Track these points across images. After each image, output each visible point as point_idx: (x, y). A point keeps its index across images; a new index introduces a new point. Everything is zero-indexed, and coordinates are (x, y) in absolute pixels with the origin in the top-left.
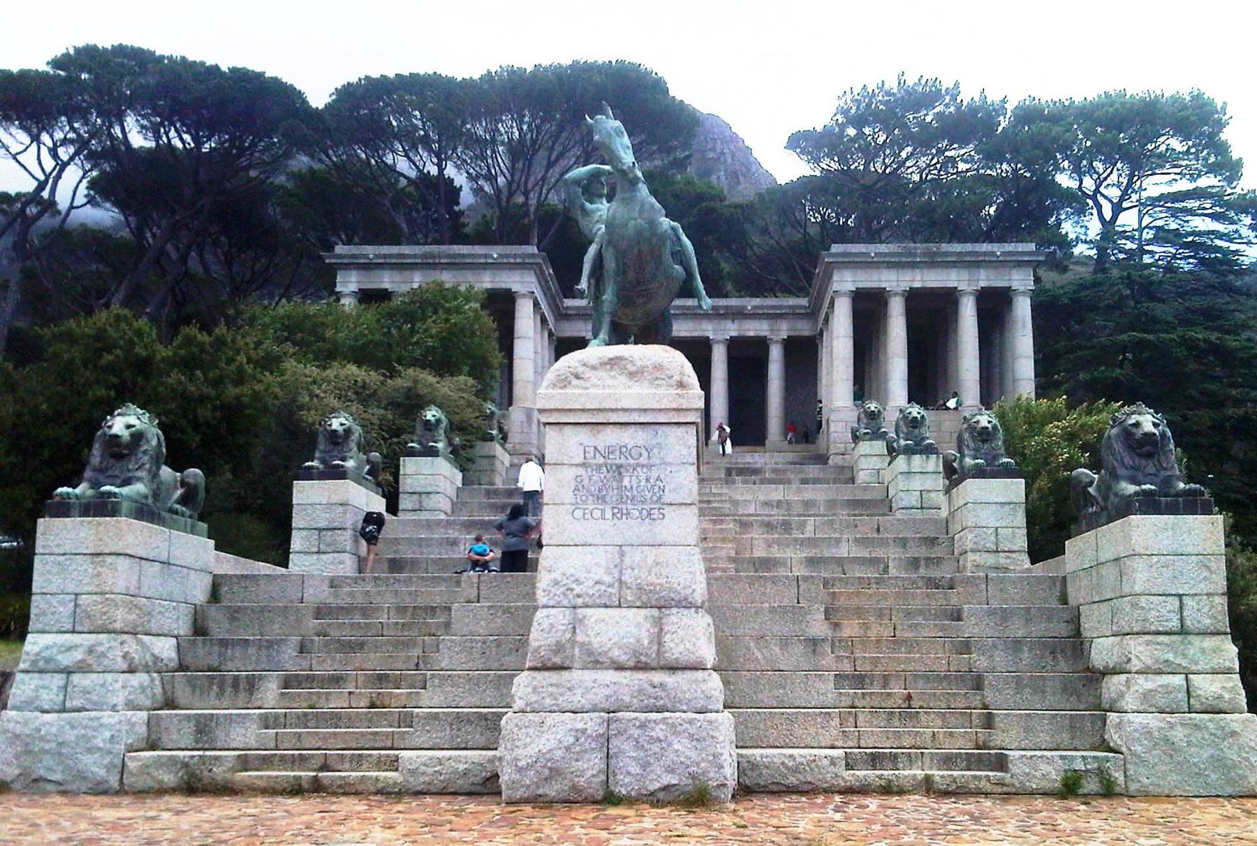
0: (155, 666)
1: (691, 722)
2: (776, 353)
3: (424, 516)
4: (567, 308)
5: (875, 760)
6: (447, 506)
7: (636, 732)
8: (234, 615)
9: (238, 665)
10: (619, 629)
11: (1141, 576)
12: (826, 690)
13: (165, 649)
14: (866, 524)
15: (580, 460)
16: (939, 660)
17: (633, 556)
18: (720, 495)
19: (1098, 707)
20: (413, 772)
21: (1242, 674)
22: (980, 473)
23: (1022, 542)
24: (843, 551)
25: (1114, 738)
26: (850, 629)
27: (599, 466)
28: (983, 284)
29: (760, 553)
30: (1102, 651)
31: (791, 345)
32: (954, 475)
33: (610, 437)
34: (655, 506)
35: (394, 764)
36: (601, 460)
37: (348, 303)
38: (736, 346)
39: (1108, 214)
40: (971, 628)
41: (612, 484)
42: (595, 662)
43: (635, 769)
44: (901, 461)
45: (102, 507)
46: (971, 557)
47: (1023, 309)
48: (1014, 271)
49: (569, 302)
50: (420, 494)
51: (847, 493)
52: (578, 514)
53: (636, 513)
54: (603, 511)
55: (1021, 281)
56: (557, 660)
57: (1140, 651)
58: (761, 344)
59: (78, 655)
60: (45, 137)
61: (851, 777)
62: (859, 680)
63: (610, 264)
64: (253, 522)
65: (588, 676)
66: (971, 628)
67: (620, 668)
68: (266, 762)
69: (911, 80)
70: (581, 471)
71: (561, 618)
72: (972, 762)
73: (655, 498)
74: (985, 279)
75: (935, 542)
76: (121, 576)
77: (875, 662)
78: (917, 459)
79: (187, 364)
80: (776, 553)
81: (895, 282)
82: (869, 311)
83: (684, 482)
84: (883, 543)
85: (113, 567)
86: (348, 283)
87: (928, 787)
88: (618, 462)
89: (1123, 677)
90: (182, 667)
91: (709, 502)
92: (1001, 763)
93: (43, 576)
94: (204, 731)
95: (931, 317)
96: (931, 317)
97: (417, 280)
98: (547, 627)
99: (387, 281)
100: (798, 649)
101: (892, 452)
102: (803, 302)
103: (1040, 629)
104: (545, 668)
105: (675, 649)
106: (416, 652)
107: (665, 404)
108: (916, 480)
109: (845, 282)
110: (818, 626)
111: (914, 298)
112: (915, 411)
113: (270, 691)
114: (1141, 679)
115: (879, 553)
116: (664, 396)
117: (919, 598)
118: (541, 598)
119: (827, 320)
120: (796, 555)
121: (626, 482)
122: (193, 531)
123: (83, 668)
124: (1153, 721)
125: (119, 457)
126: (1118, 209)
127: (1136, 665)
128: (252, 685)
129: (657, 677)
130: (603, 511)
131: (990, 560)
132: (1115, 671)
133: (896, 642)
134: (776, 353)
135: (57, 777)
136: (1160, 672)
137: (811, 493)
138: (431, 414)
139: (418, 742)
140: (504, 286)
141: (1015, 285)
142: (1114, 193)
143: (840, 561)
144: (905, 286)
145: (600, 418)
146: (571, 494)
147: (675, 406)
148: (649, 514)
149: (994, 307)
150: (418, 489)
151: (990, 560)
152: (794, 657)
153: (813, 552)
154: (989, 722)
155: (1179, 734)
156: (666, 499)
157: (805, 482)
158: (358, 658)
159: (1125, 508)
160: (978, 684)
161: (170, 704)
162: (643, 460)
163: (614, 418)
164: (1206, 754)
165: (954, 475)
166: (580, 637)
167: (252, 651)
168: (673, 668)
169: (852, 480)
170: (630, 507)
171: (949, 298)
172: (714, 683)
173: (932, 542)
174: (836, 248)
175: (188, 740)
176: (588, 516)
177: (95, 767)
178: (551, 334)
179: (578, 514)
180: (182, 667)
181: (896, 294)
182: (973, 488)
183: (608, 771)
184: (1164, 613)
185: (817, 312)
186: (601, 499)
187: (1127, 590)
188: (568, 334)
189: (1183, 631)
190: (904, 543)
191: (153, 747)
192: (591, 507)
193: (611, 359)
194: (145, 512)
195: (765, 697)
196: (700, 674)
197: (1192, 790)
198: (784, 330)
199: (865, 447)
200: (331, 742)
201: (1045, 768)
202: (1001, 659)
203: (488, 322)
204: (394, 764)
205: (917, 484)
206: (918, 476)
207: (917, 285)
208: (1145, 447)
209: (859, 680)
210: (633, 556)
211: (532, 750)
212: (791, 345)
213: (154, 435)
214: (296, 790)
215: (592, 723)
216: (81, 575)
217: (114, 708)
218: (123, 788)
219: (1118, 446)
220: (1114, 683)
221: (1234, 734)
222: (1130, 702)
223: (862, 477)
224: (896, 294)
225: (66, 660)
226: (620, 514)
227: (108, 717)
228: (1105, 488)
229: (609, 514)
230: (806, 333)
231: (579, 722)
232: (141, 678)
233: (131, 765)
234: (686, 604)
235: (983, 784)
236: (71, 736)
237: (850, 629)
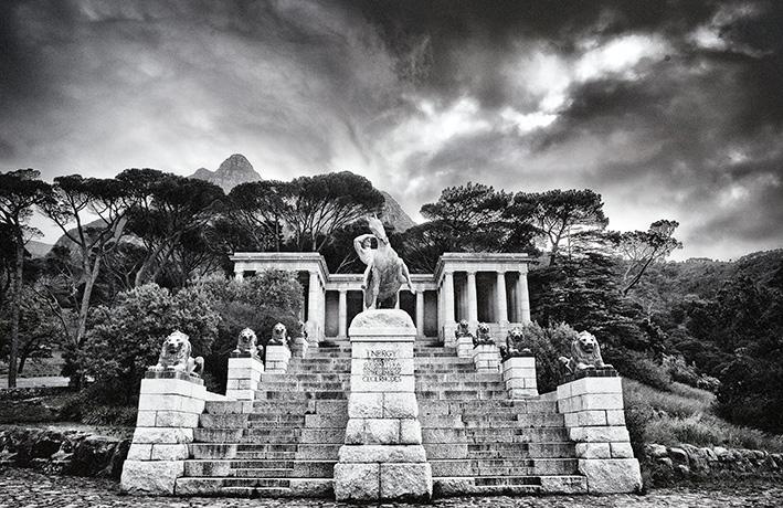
0: (186, 442)
1: (414, 467)
3: (276, 372)
5: (487, 481)
6: (285, 367)
7: (391, 471)
8: (215, 418)
9: (220, 439)
10: (384, 428)
11: (590, 402)
12: (465, 451)
13: (189, 434)
14: (469, 377)
16: (509, 437)
17: (388, 397)
19: (574, 457)
20: (296, 488)
21: (631, 441)
22: (517, 355)
23: (535, 385)
24: (460, 388)
25: (582, 469)
26: (472, 425)
29: (425, 390)
30: (575, 434)
31: (426, 293)
32: (505, 356)
33: (379, 347)
34: (395, 375)
35: (287, 484)
37: (239, 277)
39: (555, 240)
40: (521, 423)
41: (382, 367)
42: (373, 442)
43: (391, 487)
44: (480, 346)
45: (168, 374)
46: (514, 391)
47: (523, 280)
49: (331, 276)
51: (455, 361)
55: (523, 269)
56: (358, 441)
57: (592, 433)
59: (158, 437)
60: (113, 206)
61: (476, 489)
62: (478, 447)
63: (376, 275)
64: (216, 378)
65: (371, 448)
66: (521, 423)
67: (384, 444)
68: (233, 483)
71: (359, 423)
72: (526, 481)
75: (499, 385)
76: (175, 403)
77: (484, 439)
78: (486, 346)
79: (182, 306)
80: (432, 389)
81: (471, 269)
82: (460, 278)
83: (409, 365)
84: (477, 384)
85: (173, 401)
86: (239, 268)
87: (507, 492)
89: (584, 444)
90: (195, 441)
92: (538, 481)
93: (145, 402)
94: (207, 468)
95: (486, 282)
96: (486, 282)
97: (269, 266)
98: (353, 428)
99: (255, 267)
100: (451, 434)
101: (476, 344)
102: (432, 276)
103: (548, 424)
104: (353, 444)
105: (407, 437)
106: (291, 436)
108: (488, 357)
109: (449, 269)
110: (459, 424)
112: (484, 325)
113: (233, 452)
114: (592, 445)
115: (475, 389)
116: (401, 331)
117: (500, 411)
118: (350, 414)
119: (442, 283)
120: (441, 391)
122: (199, 383)
123: (159, 442)
124: (597, 462)
125: (173, 353)
126: (559, 238)
127: (589, 439)
128: (226, 449)
129: (400, 448)
131: (522, 392)
132: (580, 442)
133: (492, 430)
134: (420, 298)
135: (148, 489)
136: (599, 442)
137: (441, 360)
138: (280, 326)
139: (295, 475)
142: (557, 232)
143: (459, 393)
145: (374, 339)
149: (512, 278)
151: (522, 392)
152: (450, 438)
153: (448, 389)
154: (532, 464)
155: (608, 468)
157: (436, 355)
158: (267, 438)
159: (582, 375)
160: (525, 447)
161: (191, 457)
163: (380, 339)
164: (619, 475)
165: (505, 356)
166: (367, 431)
167: (224, 434)
168: (406, 445)
169: (456, 355)
171: (494, 275)
172: (421, 451)
173: (497, 384)
174: (445, 254)
175: (201, 473)
177: (165, 485)
180: (195, 441)
182: (514, 361)
183: (380, 488)
184: (599, 418)
185: (438, 278)
187: (585, 408)
189: (608, 425)
190: (485, 384)
191: (184, 476)
194: (184, 377)
195: (439, 455)
196: (417, 447)
197: (613, 491)
198: (423, 287)
199: (461, 340)
200: (260, 475)
201: (556, 483)
202: (535, 437)
203: (300, 287)
204: (287, 484)
205: (486, 357)
208: (587, 349)
209: (478, 447)
210: (388, 397)
211: (349, 479)
212: (426, 293)
213: (187, 344)
214: (245, 495)
215: (373, 468)
216: (159, 403)
217: (172, 460)
218: (176, 496)
219: (578, 349)
220: (580, 448)
221: (629, 467)
222: (588, 454)
223: (460, 353)
225: (152, 439)
227: (169, 463)
228: (573, 366)
231: (367, 467)
232: (181, 446)
233: (179, 484)
234: (410, 417)
235: (532, 490)
236: (153, 471)
237: (472, 425)
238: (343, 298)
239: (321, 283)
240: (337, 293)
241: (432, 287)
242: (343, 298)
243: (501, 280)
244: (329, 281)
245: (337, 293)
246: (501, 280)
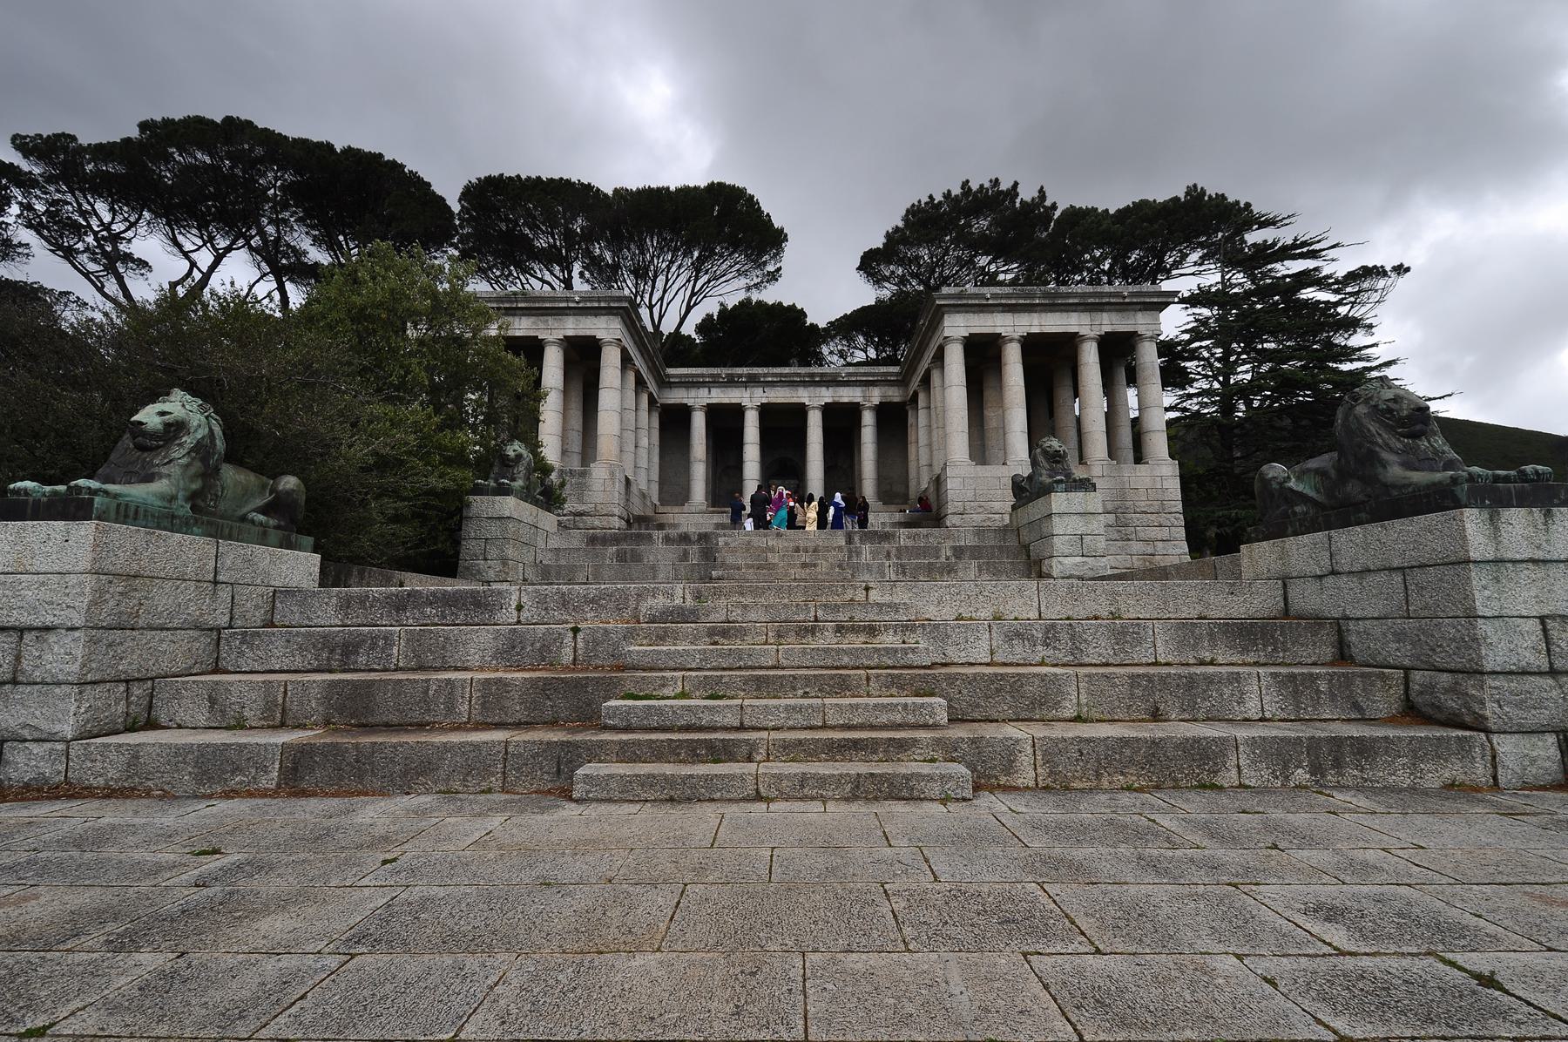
2: (868, 418)
4: (669, 376)
18: (894, 607)
28: (1108, 329)
38: (829, 411)
48: (1140, 315)
49: (671, 371)
50: (21, 631)
58: (854, 410)
69: (974, 187)
74: (1109, 323)
82: (983, 356)
91: (872, 630)
95: (1050, 362)
109: (957, 326)
111: (1033, 346)
119: (926, 381)
134: (868, 418)
140: (588, 333)
141: (1141, 330)
144: (1023, 331)
150: (26, 619)
178: (652, 401)
181: (1011, 340)
188: (672, 401)
198: (876, 396)
206: (1527, 572)
207: (1035, 330)
224: (1011, 340)
230: (896, 400)
238: (699, 422)
239: (640, 383)
240: (684, 412)
241: (895, 395)
242: (699, 422)
243: (1090, 357)
244: (664, 383)
245: (684, 412)
246: (1090, 357)
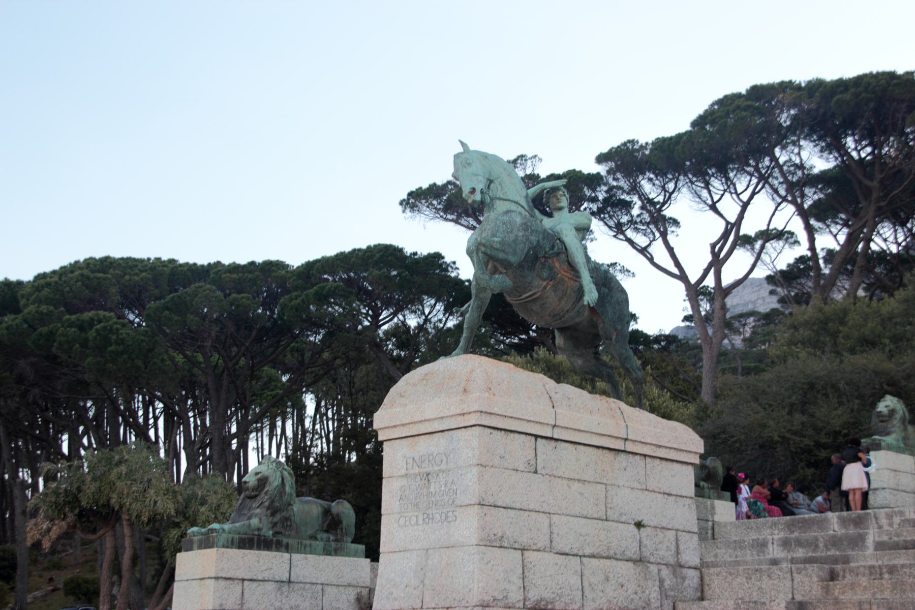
15: (403, 472)
27: (415, 475)
33: (424, 446)
36: (416, 470)
52: (402, 521)
53: (438, 516)
54: (417, 517)
70: (404, 482)
73: (450, 502)
88: (428, 470)
107: (454, 411)
121: (432, 489)
130: (417, 517)
146: (398, 503)
147: (459, 411)
148: (447, 517)
156: (458, 502)
162: (443, 466)
170: (434, 511)
176: (408, 523)
179: (402, 521)
186: (417, 505)
192: (410, 514)
193: (426, 375)
226: (429, 518)
229: (420, 522)
